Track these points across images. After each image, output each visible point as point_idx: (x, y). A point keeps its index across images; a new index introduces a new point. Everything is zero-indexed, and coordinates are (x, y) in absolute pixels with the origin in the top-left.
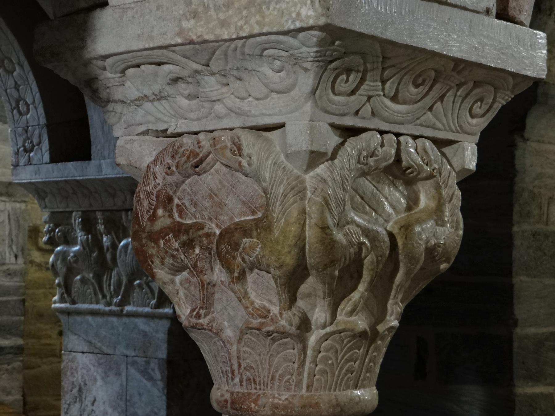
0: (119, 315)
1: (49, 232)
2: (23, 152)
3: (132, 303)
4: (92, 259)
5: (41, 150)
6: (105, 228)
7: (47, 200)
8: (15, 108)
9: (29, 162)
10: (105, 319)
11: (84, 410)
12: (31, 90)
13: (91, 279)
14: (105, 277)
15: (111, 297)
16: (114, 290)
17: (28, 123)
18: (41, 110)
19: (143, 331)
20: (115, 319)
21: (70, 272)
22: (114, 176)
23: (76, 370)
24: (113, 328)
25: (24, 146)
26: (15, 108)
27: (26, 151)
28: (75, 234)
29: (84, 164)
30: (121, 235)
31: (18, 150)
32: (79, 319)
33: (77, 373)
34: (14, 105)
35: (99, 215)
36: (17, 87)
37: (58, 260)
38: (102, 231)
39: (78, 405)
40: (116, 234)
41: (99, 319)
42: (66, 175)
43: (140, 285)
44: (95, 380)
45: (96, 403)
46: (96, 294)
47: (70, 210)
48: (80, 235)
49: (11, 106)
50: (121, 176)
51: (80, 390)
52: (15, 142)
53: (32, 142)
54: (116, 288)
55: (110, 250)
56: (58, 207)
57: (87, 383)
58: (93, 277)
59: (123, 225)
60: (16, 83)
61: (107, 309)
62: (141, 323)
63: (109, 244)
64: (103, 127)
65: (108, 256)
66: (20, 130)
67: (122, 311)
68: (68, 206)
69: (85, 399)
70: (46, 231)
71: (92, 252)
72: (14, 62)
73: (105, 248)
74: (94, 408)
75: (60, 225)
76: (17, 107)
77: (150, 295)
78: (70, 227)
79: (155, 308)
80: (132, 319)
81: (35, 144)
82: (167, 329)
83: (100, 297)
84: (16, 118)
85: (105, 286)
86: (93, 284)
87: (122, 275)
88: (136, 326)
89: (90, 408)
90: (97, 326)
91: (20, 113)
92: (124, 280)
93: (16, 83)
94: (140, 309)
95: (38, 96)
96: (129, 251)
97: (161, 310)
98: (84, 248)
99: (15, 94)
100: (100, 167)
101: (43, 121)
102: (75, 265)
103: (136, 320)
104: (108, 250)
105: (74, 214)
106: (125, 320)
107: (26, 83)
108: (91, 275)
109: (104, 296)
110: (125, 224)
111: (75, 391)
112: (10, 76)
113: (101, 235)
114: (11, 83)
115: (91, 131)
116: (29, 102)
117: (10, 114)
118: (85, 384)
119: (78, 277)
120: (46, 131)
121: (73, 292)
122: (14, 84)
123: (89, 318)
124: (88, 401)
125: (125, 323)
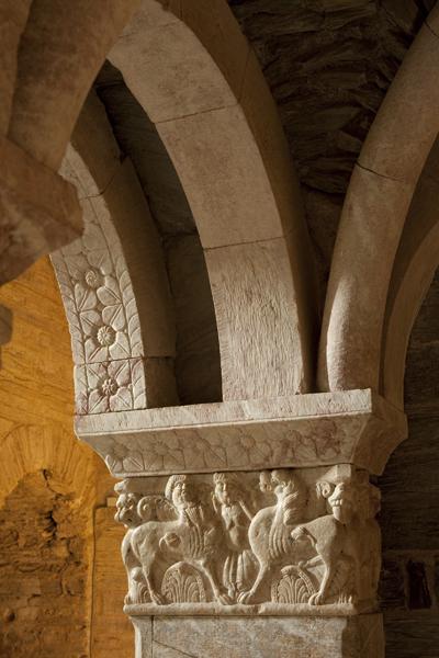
0: (252, 615)
1: (127, 503)
2: (97, 396)
3: (273, 598)
4: (205, 539)
5: (131, 391)
6: (229, 495)
7: (125, 461)
8: (88, 337)
9: (108, 409)
10: (222, 622)
12: (124, 309)
13: (203, 569)
14: (226, 563)
15: (236, 591)
16: (243, 581)
17: (109, 356)
18: (136, 338)
19: (294, 636)
20: (240, 622)
21: (162, 558)
22: (266, 421)
24: (236, 634)
25: (99, 387)
26: (88, 337)
27: (101, 394)
28: (169, 507)
29: (212, 407)
30: (254, 504)
31: (88, 394)
32: (171, 624)
34: (87, 332)
35: (217, 480)
36: (98, 308)
37: (141, 542)
38: (221, 500)
40: (245, 503)
41: (211, 624)
42: (176, 423)
43: (290, 573)
46: (207, 586)
47: (167, 473)
48: (180, 507)
49: (83, 334)
50: (281, 419)
52: (84, 382)
53: (114, 381)
54: (246, 577)
55: (237, 525)
56: (145, 470)
58: (205, 565)
59: (258, 490)
60: (99, 302)
61: (228, 608)
62: (290, 626)
63: (234, 518)
64: (245, 357)
65: (233, 535)
66: (94, 367)
67: (256, 610)
68: (163, 468)
70: (120, 504)
71: (204, 528)
72: (103, 272)
73: (228, 523)
75: (142, 496)
76: (94, 336)
77: (309, 585)
78: (160, 497)
79: (320, 604)
80: (273, 621)
81: (119, 384)
82: (340, 632)
83: (215, 591)
84: (88, 351)
85: (224, 576)
86: (202, 574)
87: (257, 560)
88: (281, 628)
90: (206, 634)
91: (97, 345)
92: (263, 567)
93: (99, 302)
94: (290, 607)
95: (134, 320)
96: (273, 526)
97: (329, 606)
98: (191, 524)
99: (94, 317)
100: (240, 411)
101: (138, 351)
102: (172, 549)
103: (281, 622)
104: (232, 525)
105: (171, 479)
106: (260, 622)
107: (118, 301)
108: (201, 562)
109: (223, 591)
110: (262, 488)
112: (92, 293)
113: (219, 505)
114: (91, 301)
115: (222, 363)
116: (115, 329)
117: (80, 345)
119: (177, 565)
120: (142, 366)
121: (164, 586)
122: (94, 304)
123: (193, 623)
125: (260, 628)
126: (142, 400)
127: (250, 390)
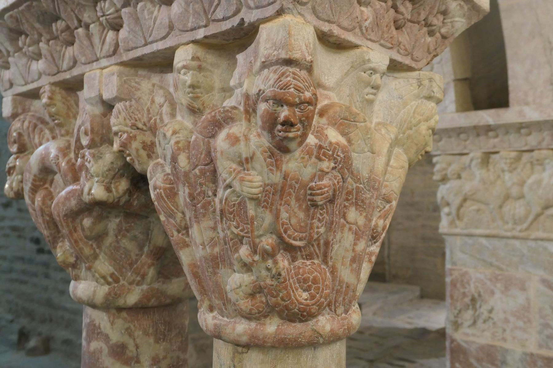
11: (478, 316)
23: (468, 283)
29: (501, 112)
33: (469, 285)
39: (470, 312)
41: (496, 242)
44: (492, 293)
45: (494, 312)
51: (473, 300)
57: (482, 293)
69: (480, 307)
74: (492, 315)
89: (486, 315)
111: (467, 300)
118: (480, 295)
123: (484, 241)
124: (484, 310)
126: (452, 107)
127: (530, 99)
